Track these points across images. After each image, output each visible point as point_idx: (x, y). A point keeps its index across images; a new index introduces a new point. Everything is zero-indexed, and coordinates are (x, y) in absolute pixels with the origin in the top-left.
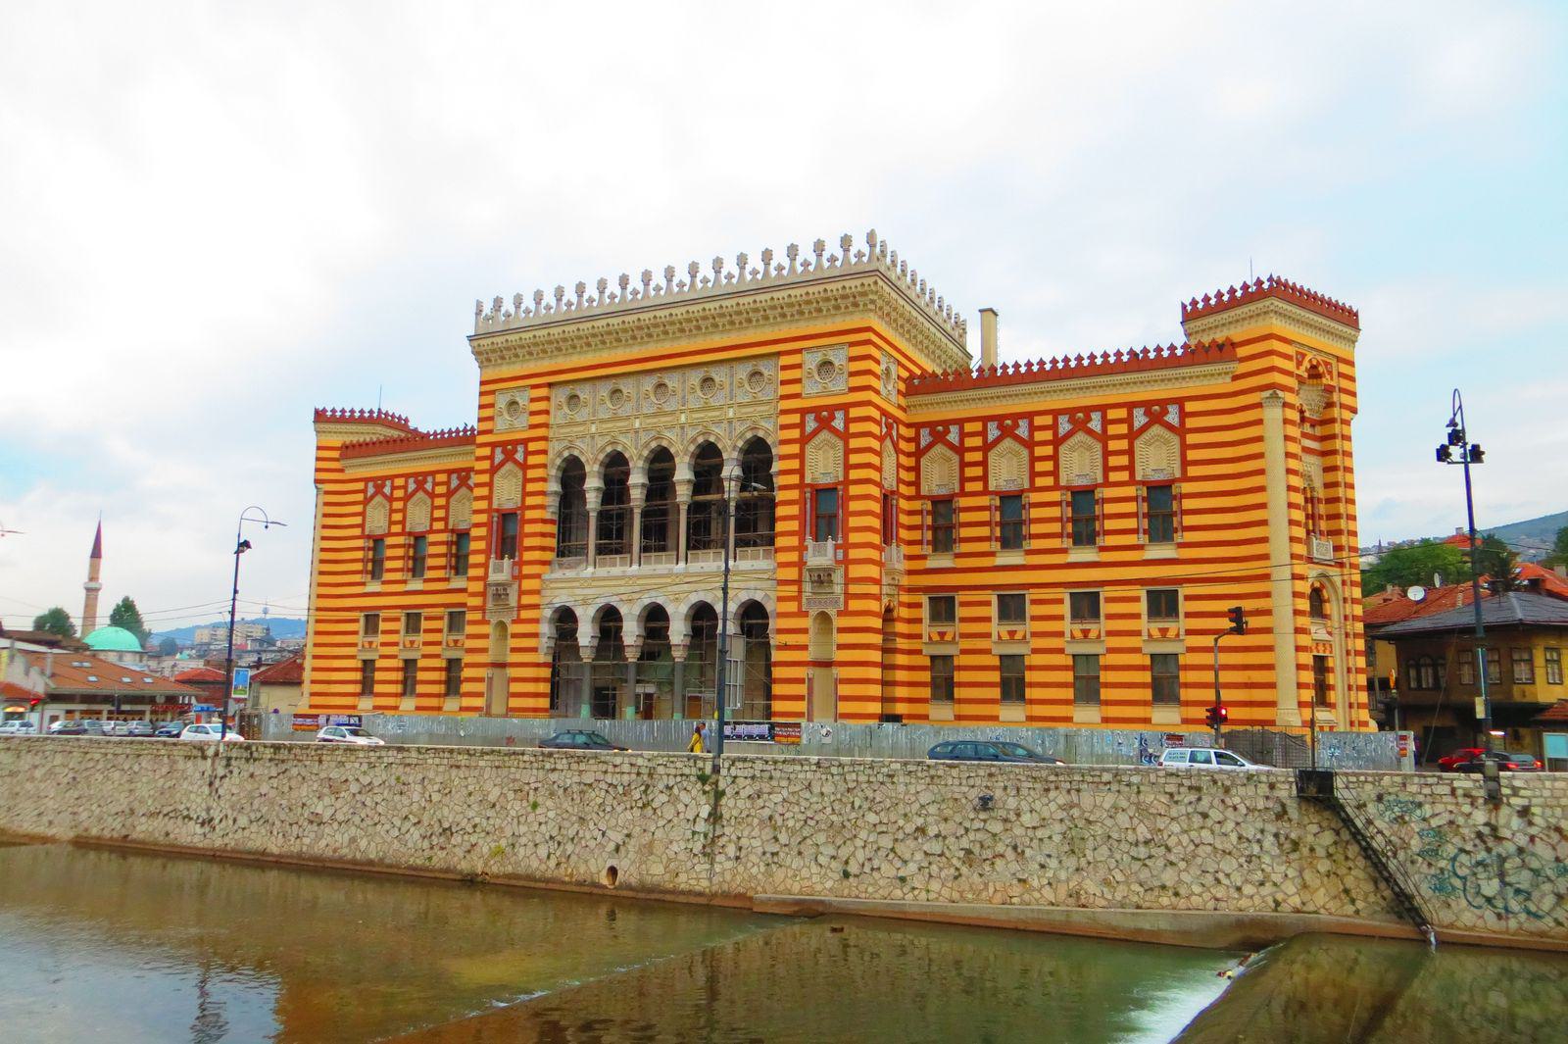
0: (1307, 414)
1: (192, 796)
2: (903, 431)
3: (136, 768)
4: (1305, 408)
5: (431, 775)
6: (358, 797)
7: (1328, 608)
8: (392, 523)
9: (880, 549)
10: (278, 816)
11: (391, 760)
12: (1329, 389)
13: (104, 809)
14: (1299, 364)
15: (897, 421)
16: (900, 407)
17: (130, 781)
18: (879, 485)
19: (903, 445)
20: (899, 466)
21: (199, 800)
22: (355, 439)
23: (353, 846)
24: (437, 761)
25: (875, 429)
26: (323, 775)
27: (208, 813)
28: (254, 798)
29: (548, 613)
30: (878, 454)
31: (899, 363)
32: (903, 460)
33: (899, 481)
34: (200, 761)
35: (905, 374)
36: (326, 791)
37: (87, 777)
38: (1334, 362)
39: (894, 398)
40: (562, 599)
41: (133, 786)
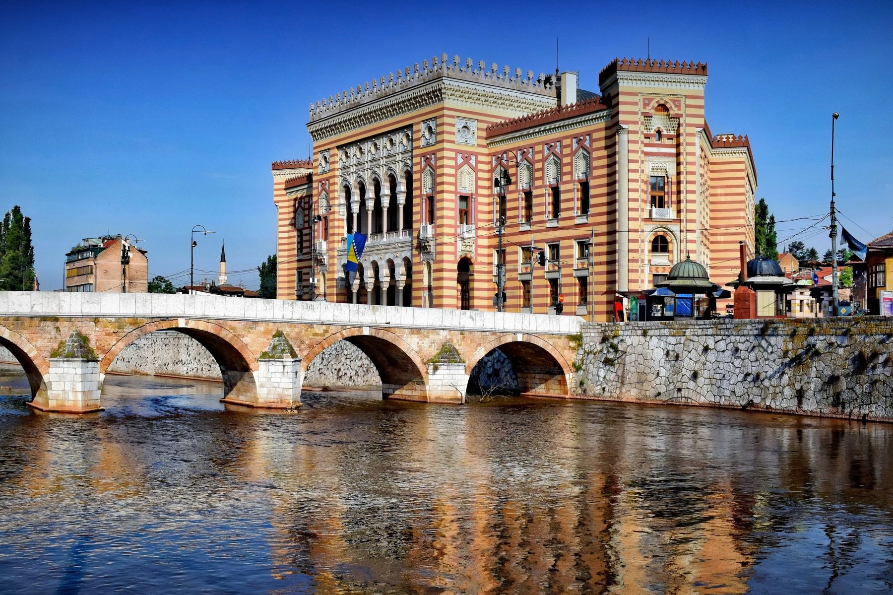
0: (665, 132)
2: (481, 158)
4: (662, 128)
7: (670, 247)
8: (305, 222)
9: (455, 227)
12: (678, 117)
14: (645, 105)
15: (476, 154)
16: (479, 146)
18: (455, 192)
19: (481, 166)
20: (477, 179)
22: (292, 176)
25: (453, 163)
30: (455, 176)
31: (478, 121)
32: (481, 175)
33: (477, 187)
35: (485, 126)
38: (683, 99)
39: (473, 141)
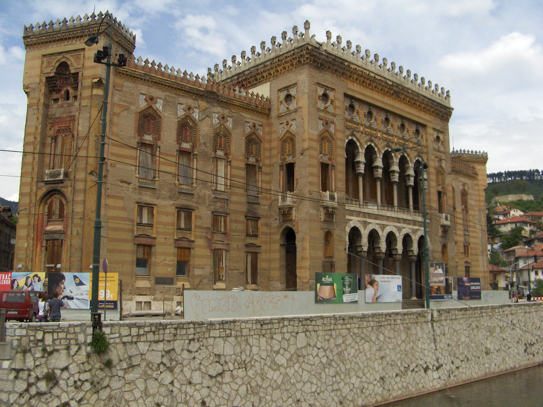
1: (426, 352)
3: (381, 337)
5: (520, 318)
6: (500, 335)
10: (473, 354)
11: (506, 312)
13: (364, 379)
17: (380, 349)
21: (430, 354)
23: (504, 362)
24: (520, 311)
26: (485, 325)
27: (438, 362)
28: (459, 346)
29: (348, 230)
34: (424, 325)
36: (488, 334)
37: (340, 354)
40: (355, 221)
41: (382, 353)
